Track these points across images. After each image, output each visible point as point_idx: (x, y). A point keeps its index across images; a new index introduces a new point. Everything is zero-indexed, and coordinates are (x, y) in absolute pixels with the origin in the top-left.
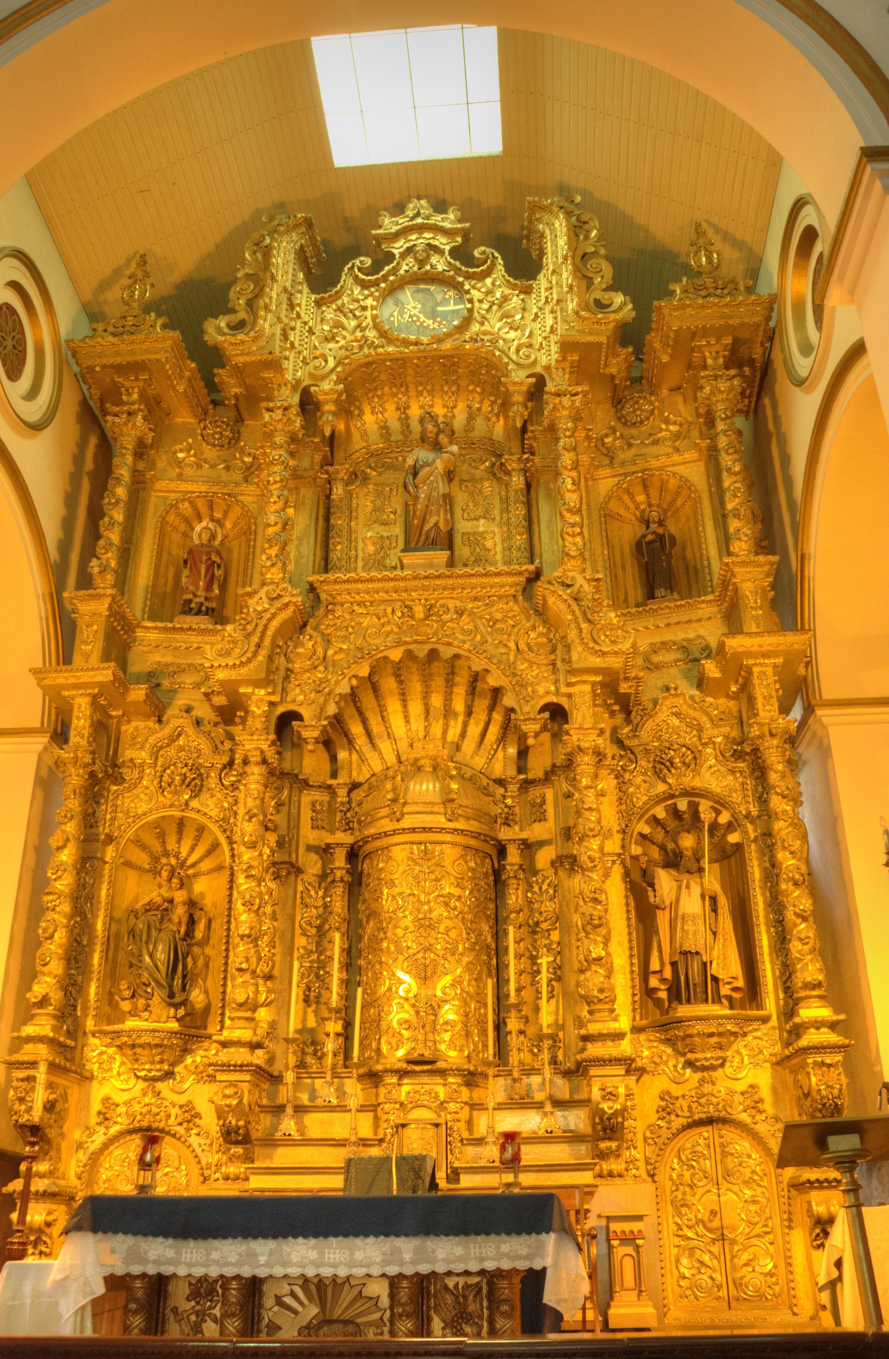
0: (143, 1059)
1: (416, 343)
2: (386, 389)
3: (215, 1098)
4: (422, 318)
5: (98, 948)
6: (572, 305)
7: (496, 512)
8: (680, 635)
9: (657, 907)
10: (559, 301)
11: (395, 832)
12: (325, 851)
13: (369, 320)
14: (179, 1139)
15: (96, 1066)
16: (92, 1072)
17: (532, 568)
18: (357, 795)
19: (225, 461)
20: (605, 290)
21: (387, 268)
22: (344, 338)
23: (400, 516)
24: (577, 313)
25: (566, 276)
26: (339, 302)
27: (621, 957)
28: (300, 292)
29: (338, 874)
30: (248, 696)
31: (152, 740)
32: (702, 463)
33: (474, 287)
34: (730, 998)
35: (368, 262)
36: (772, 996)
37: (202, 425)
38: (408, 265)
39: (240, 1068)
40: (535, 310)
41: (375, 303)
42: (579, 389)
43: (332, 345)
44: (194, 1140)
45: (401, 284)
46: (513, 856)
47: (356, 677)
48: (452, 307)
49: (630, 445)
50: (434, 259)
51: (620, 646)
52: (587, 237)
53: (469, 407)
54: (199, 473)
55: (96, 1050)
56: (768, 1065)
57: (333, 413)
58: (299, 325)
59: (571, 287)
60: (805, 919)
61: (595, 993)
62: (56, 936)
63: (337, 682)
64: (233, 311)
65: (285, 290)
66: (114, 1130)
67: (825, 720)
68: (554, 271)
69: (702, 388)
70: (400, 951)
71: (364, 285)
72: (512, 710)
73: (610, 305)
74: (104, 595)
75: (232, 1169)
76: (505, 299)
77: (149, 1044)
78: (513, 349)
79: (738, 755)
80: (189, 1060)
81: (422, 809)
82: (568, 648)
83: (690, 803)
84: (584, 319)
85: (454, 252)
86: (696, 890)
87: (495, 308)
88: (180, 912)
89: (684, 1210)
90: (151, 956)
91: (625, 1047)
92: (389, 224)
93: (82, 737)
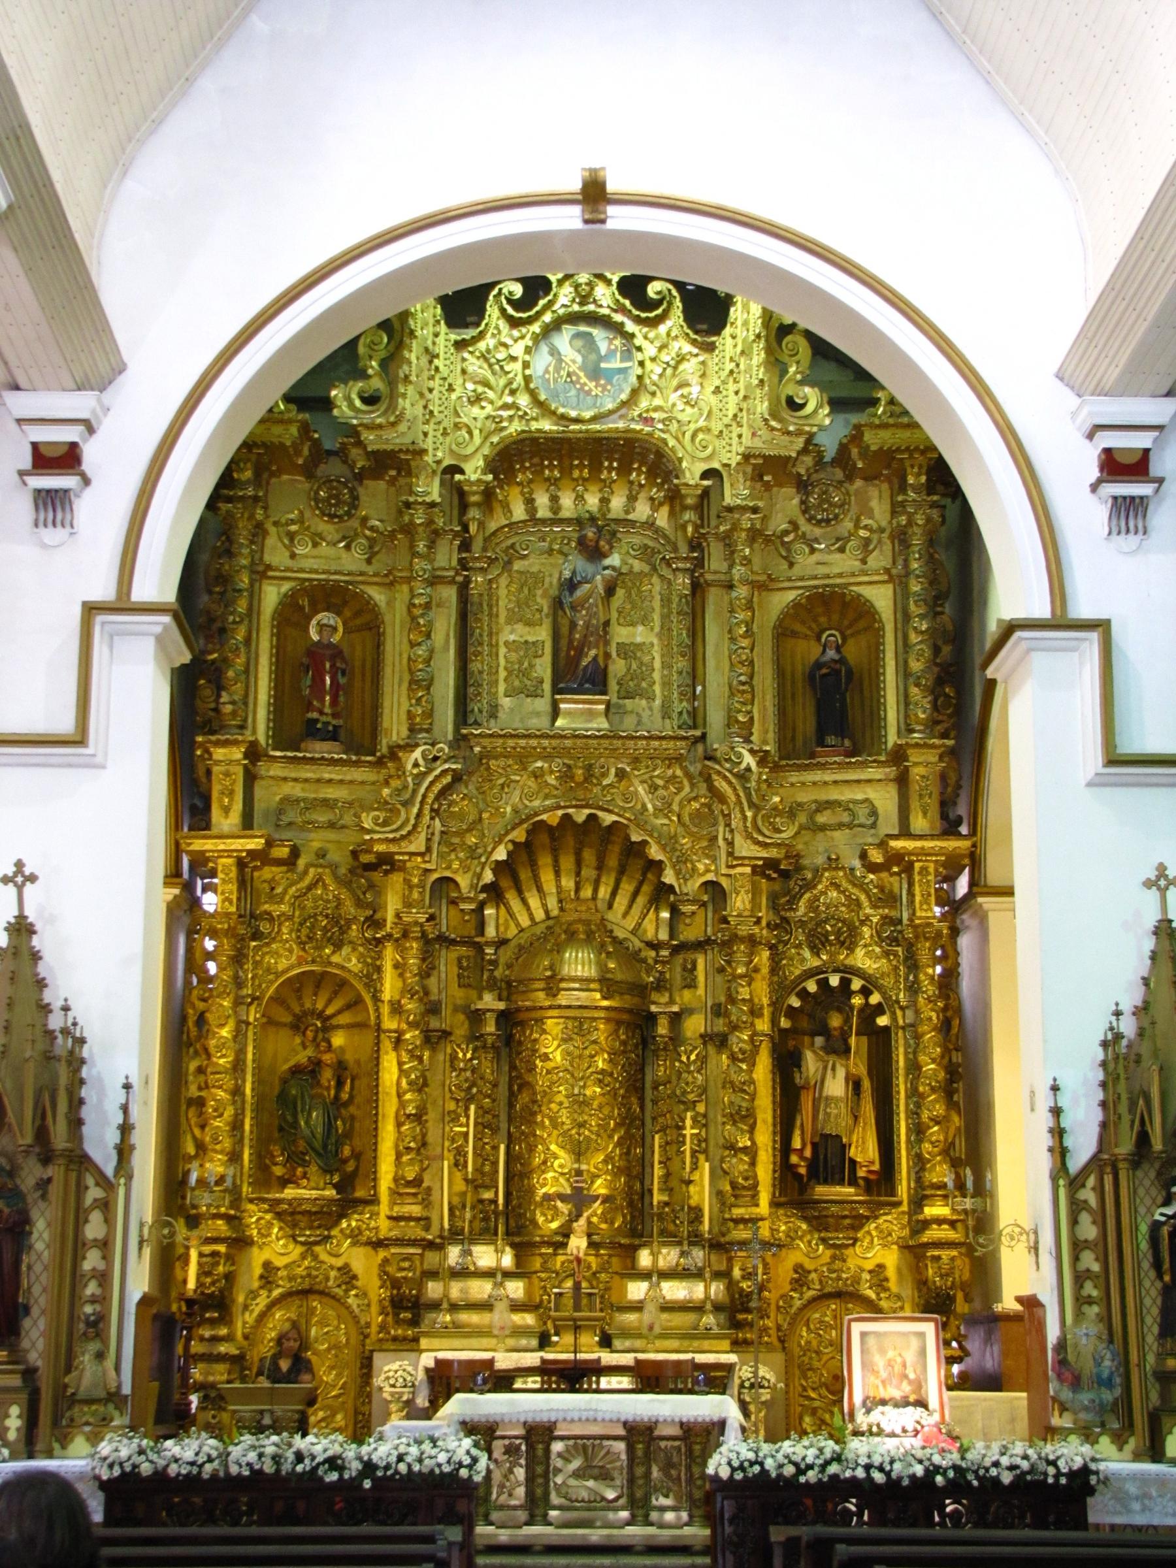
0: (302, 1225)
1: (577, 421)
2: (536, 460)
3: (389, 1269)
4: (584, 380)
5: (248, 1114)
6: (762, 407)
7: (656, 617)
9: (803, 1087)
10: (745, 398)
11: (550, 1007)
12: (476, 1017)
14: (338, 1300)
15: (255, 1232)
16: (251, 1236)
17: (698, 733)
18: (506, 955)
19: (344, 538)
21: (542, 303)
22: (492, 402)
23: (547, 616)
24: (766, 420)
26: (481, 346)
27: (764, 1137)
29: (490, 1040)
30: (405, 862)
31: (292, 890)
32: (891, 586)
34: (864, 1178)
36: (904, 1183)
39: (413, 1243)
40: (717, 383)
43: (475, 411)
45: (557, 325)
46: (662, 1029)
47: (512, 841)
48: (616, 364)
49: (813, 550)
51: (783, 835)
54: (315, 552)
55: (255, 1216)
56: (895, 1247)
58: (437, 382)
59: (762, 381)
60: (937, 1123)
61: (740, 1180)
62: (226, 1115)
63: (494, 849)
65: (427, 350)
66: (276, 1293)
67: (985, 906)
68: (743, 353)
70: (555, 1124)
71: (514, 323)
72: (671, 888)
73: (802, 406)
75: (400, 1332)
76: (681, 359)
77: (309, 1212)
79: (894, 941)
80: (344, 1224)
81: (577, 985)
82: (732, 831)
83: (842, 979)
84: (773, 429)
86: (841, 1073)
87: (669, 371)
88: (327, 1076)
89: (810, 1373)
90: (307, 1123)
91: (765, 1232)
93: (231, 903)
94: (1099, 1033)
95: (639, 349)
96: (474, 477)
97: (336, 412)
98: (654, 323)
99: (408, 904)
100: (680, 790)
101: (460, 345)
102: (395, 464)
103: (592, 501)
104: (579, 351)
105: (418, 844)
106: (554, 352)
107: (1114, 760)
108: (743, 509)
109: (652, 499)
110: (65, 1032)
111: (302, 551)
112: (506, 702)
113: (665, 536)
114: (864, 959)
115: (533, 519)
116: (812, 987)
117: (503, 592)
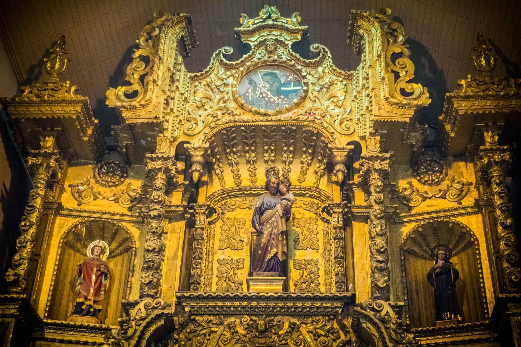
1: (265, 114)
2: (240, 147)
4: (270, 95)
10: (373, 89)
13: (230, 94)
17: (349, 294)
20: (409, 82)
21: (244, 56)
22: (211, 108)
23: (247, 244)
24: (387, 99)
25: (380, 69)
26: (208, 80)
28: (179, 71)
32: (480, 216)
33: (309, 74)
35: (231, 50)
37: (99, 166)
38: (260, 55)
40: (355, 93)
41: (235, 82)
42: (387, 155)
43: (201, 112)
48: (292, 88)
49: (425, 199)
50: (280, 51)
52: (395, 41)
53: (302, 163)
54: (94, 203)
57: (200, 163)
58: (177, 95)
59: (383, 79)
64: (129, 84)
65: (169, 69)
68: (370, 66)
69: (481, 158)
71: (228, 68)
73: (412, 94)
74: (17, 299)
76: (332, 83)
78: (337, 123)
84: (392, 104)
85: (296, 47)
87: (325, 90)
92: (248, 23)
96: (197, 145)
97: (107, 103)
100: (339, 338)
104: (268, 82)
108: (376, 158)
109: (316, 173)
113: (325, 195)
117: (218, 230)
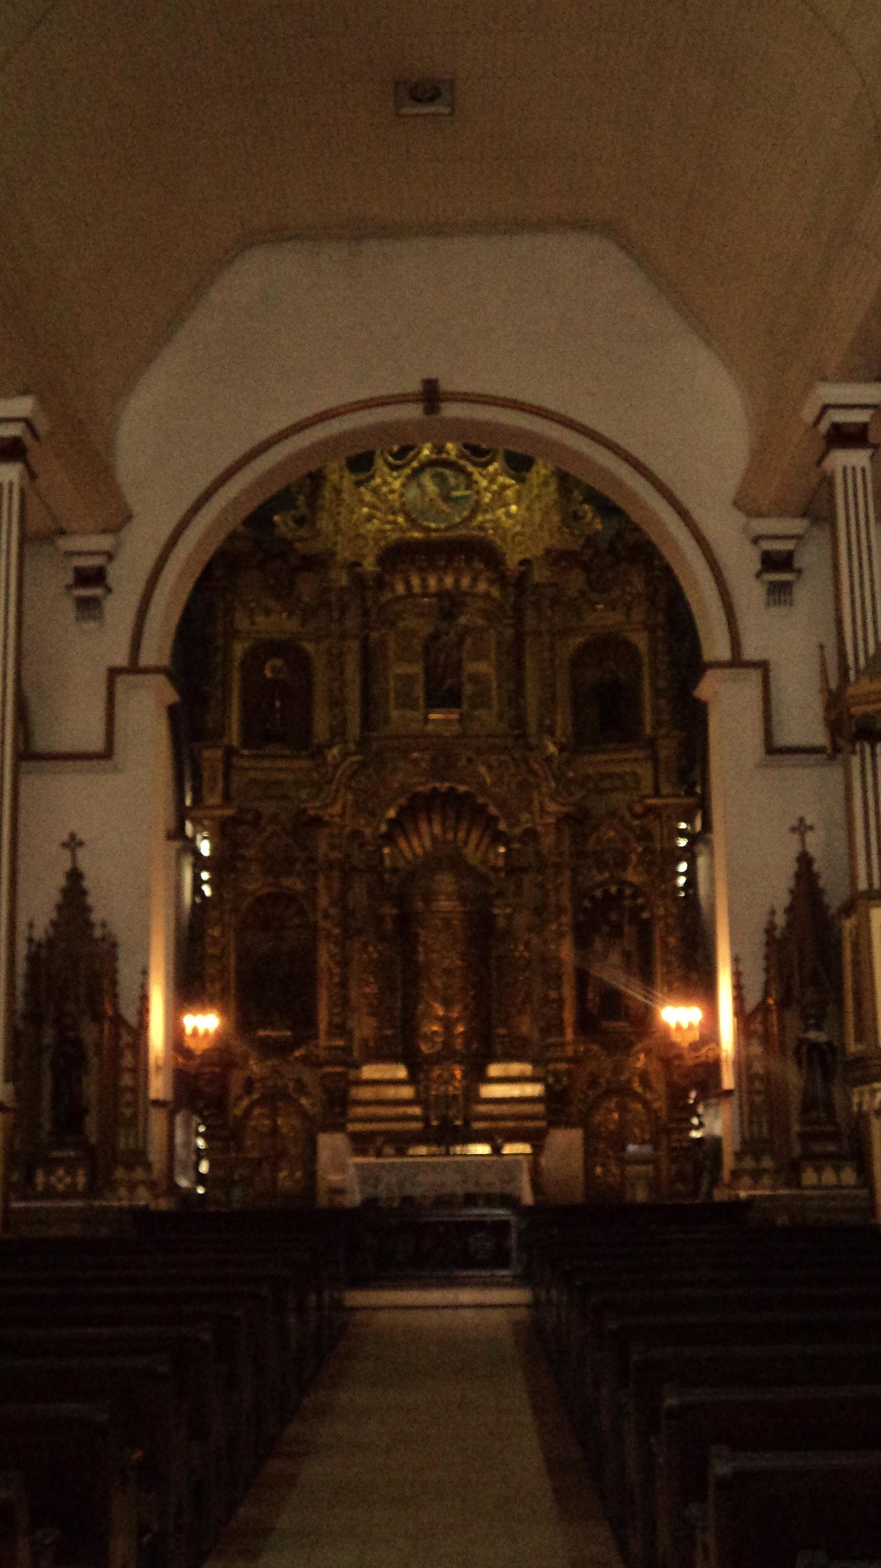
1: (436, 530)
6: (556, 518)
8: (618, 769)
27: (568, 992)
44: (304, 1101)
46: (501, 923)
66: (255, 1096)
71: (393, 468)
78: (509, 537)
94: (763, 925)
95: (476, 482)
98: (485, 465)
99: (333, 847)
101: (359, 484)
102: (318, 563)
103: (449, 581)
105: (337, 809)
106: (420, 486)
107: (773, 749)
110: (104, 939)
111: (262, 620)
112: (395, 714)
114: (632, 876)
115: (410, 594)
116: (598, 893)
